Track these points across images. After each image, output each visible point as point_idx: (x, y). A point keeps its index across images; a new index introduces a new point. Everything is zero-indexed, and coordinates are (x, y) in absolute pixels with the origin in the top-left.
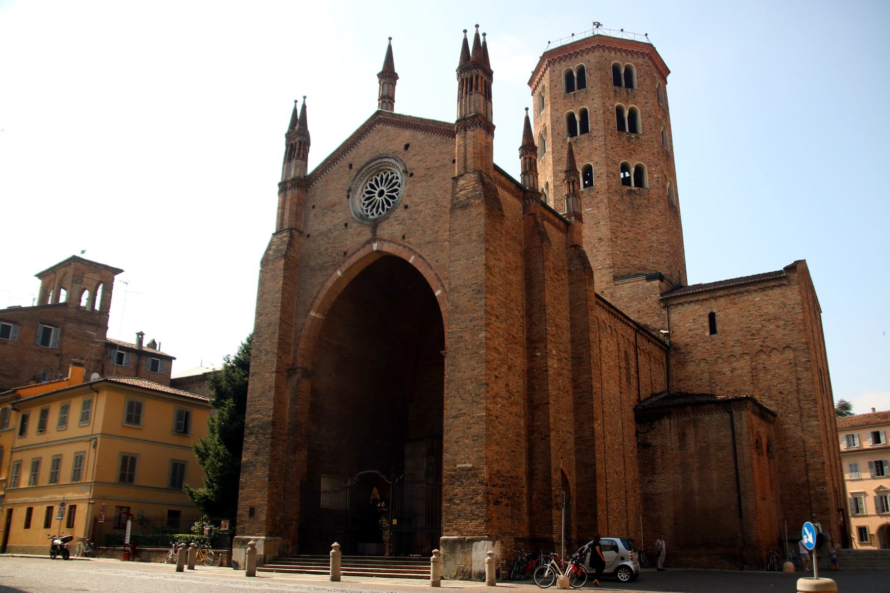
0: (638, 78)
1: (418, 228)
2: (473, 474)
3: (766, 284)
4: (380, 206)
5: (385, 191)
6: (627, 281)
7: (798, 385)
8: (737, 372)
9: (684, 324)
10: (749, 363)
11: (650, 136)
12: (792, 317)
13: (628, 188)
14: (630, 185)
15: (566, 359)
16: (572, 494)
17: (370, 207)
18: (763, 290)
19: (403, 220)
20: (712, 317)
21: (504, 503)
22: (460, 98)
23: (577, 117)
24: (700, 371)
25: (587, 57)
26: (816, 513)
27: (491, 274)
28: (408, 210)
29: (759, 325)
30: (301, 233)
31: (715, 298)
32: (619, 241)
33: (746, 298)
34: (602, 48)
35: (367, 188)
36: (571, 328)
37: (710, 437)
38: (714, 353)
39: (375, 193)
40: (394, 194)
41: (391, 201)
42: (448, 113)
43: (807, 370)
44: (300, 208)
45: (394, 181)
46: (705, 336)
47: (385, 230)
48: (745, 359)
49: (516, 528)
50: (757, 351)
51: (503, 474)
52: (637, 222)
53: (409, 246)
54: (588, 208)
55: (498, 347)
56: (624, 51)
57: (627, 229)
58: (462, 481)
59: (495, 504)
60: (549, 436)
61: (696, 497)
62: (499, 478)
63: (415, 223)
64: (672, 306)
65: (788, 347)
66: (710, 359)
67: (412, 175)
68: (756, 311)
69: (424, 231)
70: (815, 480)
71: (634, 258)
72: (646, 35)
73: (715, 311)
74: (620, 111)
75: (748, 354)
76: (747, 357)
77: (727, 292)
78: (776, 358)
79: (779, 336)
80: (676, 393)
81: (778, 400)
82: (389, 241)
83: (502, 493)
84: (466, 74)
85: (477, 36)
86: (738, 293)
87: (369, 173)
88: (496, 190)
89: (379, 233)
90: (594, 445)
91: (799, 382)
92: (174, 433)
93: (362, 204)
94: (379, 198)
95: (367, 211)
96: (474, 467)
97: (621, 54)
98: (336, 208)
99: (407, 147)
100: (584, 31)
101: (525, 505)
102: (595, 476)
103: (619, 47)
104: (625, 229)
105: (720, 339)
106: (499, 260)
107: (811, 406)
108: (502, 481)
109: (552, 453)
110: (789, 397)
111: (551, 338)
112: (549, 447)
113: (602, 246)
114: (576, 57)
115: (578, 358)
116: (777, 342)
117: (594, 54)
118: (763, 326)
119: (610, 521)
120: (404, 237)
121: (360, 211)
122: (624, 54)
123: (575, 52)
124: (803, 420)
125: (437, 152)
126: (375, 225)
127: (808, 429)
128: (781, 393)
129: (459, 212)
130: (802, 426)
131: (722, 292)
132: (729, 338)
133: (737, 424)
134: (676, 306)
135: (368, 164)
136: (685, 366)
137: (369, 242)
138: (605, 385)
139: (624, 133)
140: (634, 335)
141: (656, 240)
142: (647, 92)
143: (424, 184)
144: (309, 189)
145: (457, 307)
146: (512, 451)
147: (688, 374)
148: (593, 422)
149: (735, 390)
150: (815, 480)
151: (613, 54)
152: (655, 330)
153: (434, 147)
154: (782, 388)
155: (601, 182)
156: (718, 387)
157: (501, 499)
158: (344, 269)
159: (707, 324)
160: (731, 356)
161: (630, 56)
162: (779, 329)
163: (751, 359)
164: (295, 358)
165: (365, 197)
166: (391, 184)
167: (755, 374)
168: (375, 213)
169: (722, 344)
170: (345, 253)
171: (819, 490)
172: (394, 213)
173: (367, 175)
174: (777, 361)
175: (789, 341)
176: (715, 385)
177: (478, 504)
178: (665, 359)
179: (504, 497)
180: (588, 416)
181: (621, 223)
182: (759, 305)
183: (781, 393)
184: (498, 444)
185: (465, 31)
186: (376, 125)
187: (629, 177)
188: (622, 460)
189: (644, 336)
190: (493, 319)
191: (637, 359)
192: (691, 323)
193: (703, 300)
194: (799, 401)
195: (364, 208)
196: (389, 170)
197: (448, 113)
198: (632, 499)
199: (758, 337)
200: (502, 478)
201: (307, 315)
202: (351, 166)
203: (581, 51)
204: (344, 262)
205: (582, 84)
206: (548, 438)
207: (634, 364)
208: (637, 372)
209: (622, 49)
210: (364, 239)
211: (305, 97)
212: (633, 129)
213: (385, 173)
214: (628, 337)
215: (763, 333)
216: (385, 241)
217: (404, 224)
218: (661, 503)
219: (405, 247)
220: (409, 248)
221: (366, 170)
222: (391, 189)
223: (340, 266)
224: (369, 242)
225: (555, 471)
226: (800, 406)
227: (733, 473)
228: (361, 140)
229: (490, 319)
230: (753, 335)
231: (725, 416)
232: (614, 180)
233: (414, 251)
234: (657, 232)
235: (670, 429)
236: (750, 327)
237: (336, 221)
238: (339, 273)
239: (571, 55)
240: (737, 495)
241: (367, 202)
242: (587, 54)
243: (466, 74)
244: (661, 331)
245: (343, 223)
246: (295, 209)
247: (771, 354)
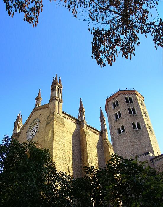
19: (38, 136)
23: (118, 114)
25: (119, 97)
74: (129, 109)
104: (136, 142)
113: (130, 148)
143: (43, 123)
151: (125, 95)
205: (117, 104)
212: (134, 113)
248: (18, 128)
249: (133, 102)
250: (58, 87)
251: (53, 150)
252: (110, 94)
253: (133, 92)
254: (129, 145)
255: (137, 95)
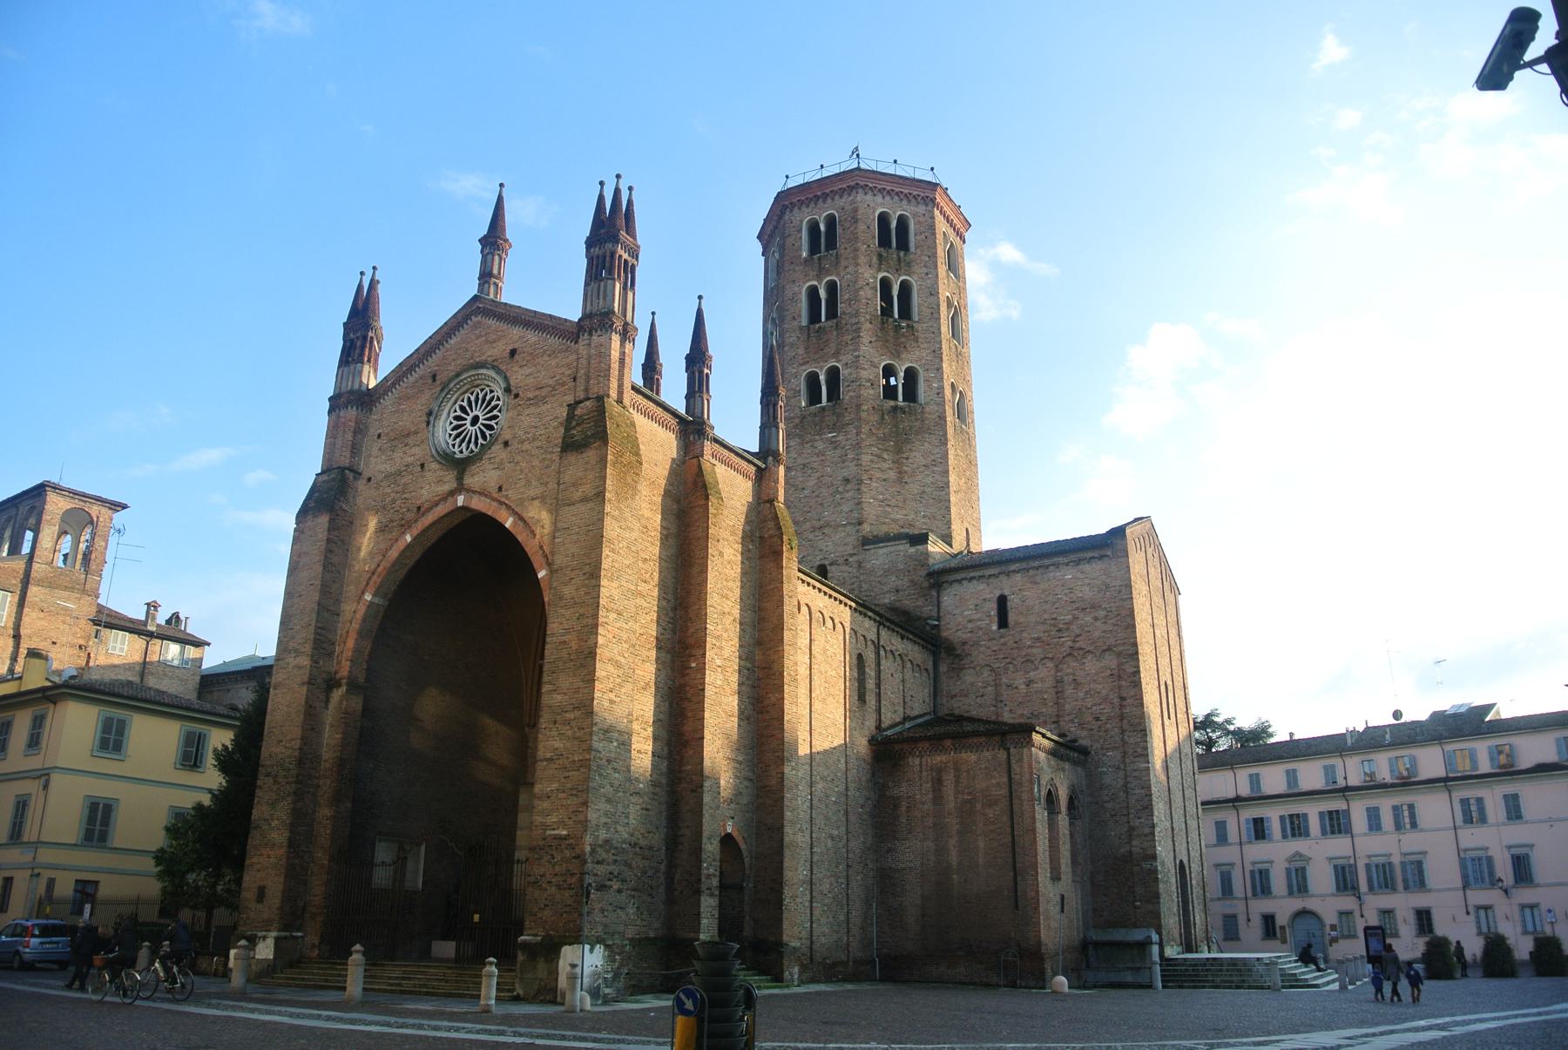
0: (916, 235)
1: (521, 477)
2: (568, 845)
3: (1080, 555)
4: (473, 440)
5: (481, 418)
6: (882, 545)
7: (1122, 706)
8: (1035, 685)
9: (964, 611)
10: (1053, 672)
11: (930, 324)
12: (1117, 604)
13: (892, 403)
14: (895, 398)
15: (748, 669)
16: (747, 872)
17: (458, 440)
18: (1079, 562)
19: (501, 463)
20: (1002, 602)
21: (615, 887)
22: (587, 284)
23: (823, 294)
24: (983, 683)
26: (1141, 901)
27: (613, 551)
28: (509, 449)
29: (1070, 617)
30: (358, 474)
31: (1008, 574)
32: (874, 484)
33: (1052, 574)
34: (864, 190)
35: (455, 411)
36: (758, 623)
37: (977, 786)
38: (1002, 656)
39: (466, 419)
40: (492, 423)
41: (488, 433)
42: (571, 309)
43: (1136, 686)
44: (359, 436)
45: (493, 403)
46: (991, 631)
47: (473, 479)
48: (1047, 667)
49: (644, 923)
50: (1065, 654)
51: (615, 845)
52: (904, 456)
53: (506, 502)
54: (830, 433)
55: (619, 658)
56: (897, 194)
57: (887, 466)
58: (552, 855)
59: (597, 890)
60: (702, 786)
61: (954, 876)
62: (608, 851)
63: (518, 468)
64: (945, 585)
65: (1109, 649)
66: (997, 665)
67: (517, 396)
68: (1066, 595)
69: (529, 481)
70: (1141, 851)
71: (896, 509)
72: (932, 169)
73: (1006, 593)
74: (885, 285)
75: (1052, 659)
76: (1050, 665)
77: (1024, 565)
78: (1091, 665)
79: (1097, 634)
80: (947, 715)
81: (1093, 729)
82: (481, 494)
83: (611, 873)
84: (597, 249)
85: (617, 192)
86: (1041, 566)
87: (459, 389)
88: (633, 424)
89: (468, 480)
90: (783, 798)
91: (1124, 703)
92: (179, 766)
93: (448, 435)
94: (471, 428)
95: (454, 445)
96: (569, 835)
97: (892, 199)
98: (410, 440)
99: (513, 352)
100: (839, 162)
101: (662, 889)
102: (782, 845)
103: (888, 188)
104: (886, 465)
105: (1013, 635)
106: (632, 530)
107: (1139, 740)
108: (613, 855)
109: (704, 812)
110: (1109, 726)
111: (714, 642)
112: (700, 803)
113: (847, 491)
114: (824, 202)
115: (765, 668)
116: (1094, 643)
117: (850, 199)
118: (1073, 615)
119: (816, 913)
120: (500, 489)
121: (444, 445)
122: (896, 197)
123: (823, 194)
124: (1127, 761)
125: (553, 363)
126: (460, 466)
127: (1134, 774)
128: (1097, 719)
129: (572, 458)
130: (1125, 770)
131: (1018, 565)
132: (1025, 635)
133: (1015, 766)
134: (951, 584)
135: (458, 375)
136: (961, 675)
137: (453, 493)
138: (817, 706)
139: (891, 320)
140: (875, 630)
141: (932, 483)
142: (929, 257)
143: (532, 410)
144: (374, 409)
145: (561, 598)
146: (642, 809)
147: (964, 687)
148: (783, 764)
149: (1032, 714)
150: (1141, 851)
151: (879, 199)
152: (919, 618)
153: (549, 356)
154: (1098, 711)
155: (852, 394)
156: (1007, 709)
157: (610, 883)
158: (416, 532)
159: (994, 613)
160: (1027, 661)
161: (905, 202)
162: (1098, 624)
163: (1057, 666)
164: (339, 663)
165: (452, 425)
166: (489, 408)
167: (1060, 690)
168: (464, 450)
169: (1016, 642)
170: (419, 508)
171: (1146, 866)
172: (489, 452)
173: (456, 392)
174: (1094, 672)
175: (1112, 641)
176: (1003, 705)
177: (573, 889)
178: (931, 663)
179: (615, 880)
180: (777, 754)
181: (879, 456)
182: (1071, 586)
183: (1097, 719)
184: (609, 801)
185: (602, 183)
186: (473, 317)
187: (896, 386)
188: (844, 819)
189: (893, 630)
190: (613, 616)
191: (878, 664)
192: (971, 610)
193: (990, 576)
194: (1123, 732)
195: (451, 442)
196: (488, 386)
197: (571, 309)
198: (859, 878)
199: (1067, 634)
200: (613, 851)
201: (360, 599)
202: (434, 377)
203: (831, 192)
204: (416, 521)
205: (832, 242)
206: (700, 790)
207: (873, 674)
208: (878, 686)
209: (893, 190)
210: (447, 487)
211: (374, 268)
212: (906, 312)
213: (482, 390)
214: (865, 633)
215: (1074, 627)
216: (474, 492)
217: (502, 469)
218: (903, 883)
219: (501, 503)
220: (506, 505)
221: (456, 385)
222: (488, 415)
223: (410, 527)
224: (453, 493)
225: (709, 839)
226: (1123, 739)
227: (1008, 839)
228: (451, 338)
229: (607, 617)
230: (1060, 630)
231: (999, 755)
232: (872, 392)
233: (513, 510)
234: (933, 472)
235: (921, 771)
236: (1056, 619)
237: (410, 460)
238: (409, 538)
239: (817, 198)
240: (1012, 874)
241: (455, 432)
242: (841, 197)
243: (597, 249)
244: (929, 621)
245: (419, 463)
246: (351, 439)
247: (1084, 660)
248: (369, 361)
249: (912, 248)
250: (625, 256)
251: (602, 583)
252: (804, 171)
253: (925, 192)
254: (845, 473)
255: (937, 212)
